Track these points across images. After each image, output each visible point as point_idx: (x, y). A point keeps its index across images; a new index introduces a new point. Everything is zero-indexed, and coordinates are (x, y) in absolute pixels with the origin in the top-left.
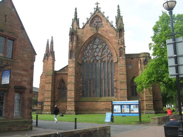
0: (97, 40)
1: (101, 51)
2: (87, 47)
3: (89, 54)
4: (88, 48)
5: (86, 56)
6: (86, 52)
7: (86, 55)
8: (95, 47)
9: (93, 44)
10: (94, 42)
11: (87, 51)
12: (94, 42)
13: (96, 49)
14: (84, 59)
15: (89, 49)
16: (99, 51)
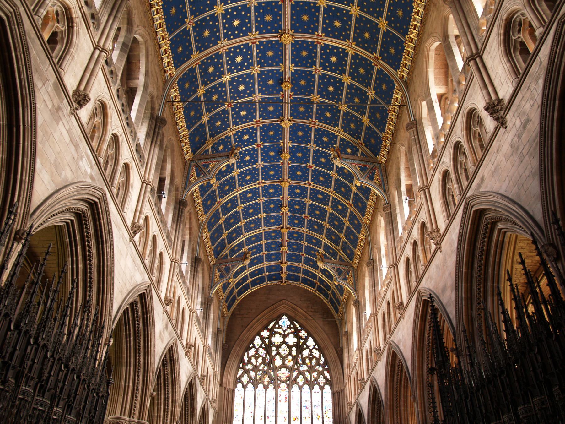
0: (285, 322)
1: (294, 353)
2: (254, 340)
3: (260, 360)
4: (257, 342)
5: (249, 367)
6: (250, 355)
7: (252, 364)
8: (277, 339)
9: (272, 333)
10: (274, 327)
11: (252, 352)
12: (274, 327)
13: (278, 347)
14: (242, 376)
15: (261, 346)
16: (290, 354)
